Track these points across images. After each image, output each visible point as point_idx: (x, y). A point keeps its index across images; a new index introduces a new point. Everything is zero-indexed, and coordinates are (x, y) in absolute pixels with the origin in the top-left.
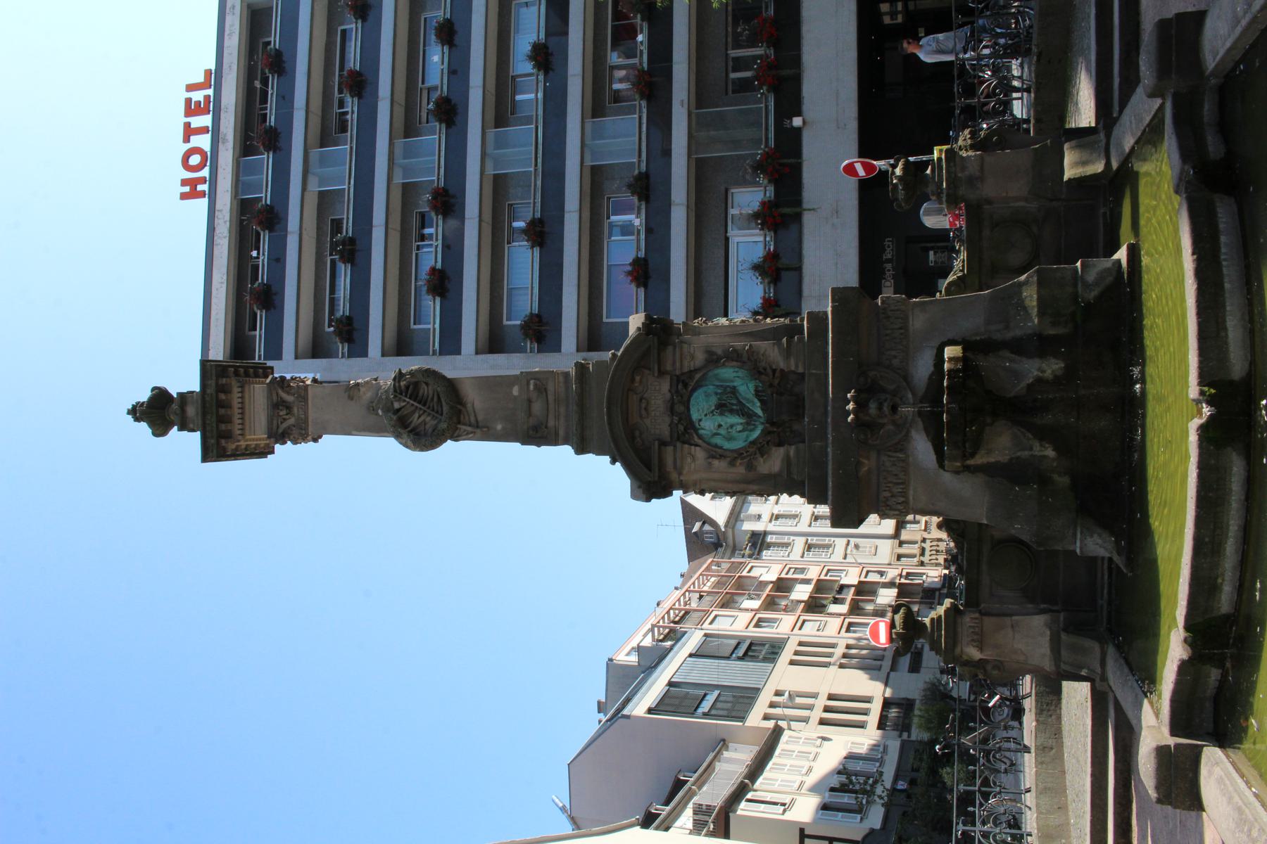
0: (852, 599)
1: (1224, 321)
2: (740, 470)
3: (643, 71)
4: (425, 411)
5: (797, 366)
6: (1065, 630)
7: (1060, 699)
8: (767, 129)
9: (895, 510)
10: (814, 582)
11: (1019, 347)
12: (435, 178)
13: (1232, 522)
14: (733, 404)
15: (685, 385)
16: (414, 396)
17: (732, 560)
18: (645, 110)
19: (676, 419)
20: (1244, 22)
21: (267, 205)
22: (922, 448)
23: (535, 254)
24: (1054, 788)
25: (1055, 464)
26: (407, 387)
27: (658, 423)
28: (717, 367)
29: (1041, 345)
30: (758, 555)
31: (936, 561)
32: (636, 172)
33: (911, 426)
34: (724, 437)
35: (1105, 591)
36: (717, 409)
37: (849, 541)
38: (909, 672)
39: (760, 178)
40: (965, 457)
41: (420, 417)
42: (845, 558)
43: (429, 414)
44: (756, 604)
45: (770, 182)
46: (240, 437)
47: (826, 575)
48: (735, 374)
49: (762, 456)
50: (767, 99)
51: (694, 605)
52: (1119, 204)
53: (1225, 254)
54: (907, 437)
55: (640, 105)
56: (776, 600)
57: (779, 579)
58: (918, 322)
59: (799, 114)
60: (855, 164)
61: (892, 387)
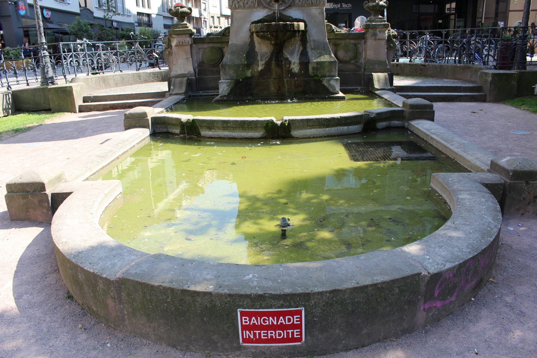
1: (314, 128)
6: (188, 79)
7: (160, 81)
9: (232, 4)
11: (304, 54)
13: (236, 133)
22: (260, 14)
24: (124, 82)
29: (304, 63)
33: (269, 9)
35: (205, 94)
38: (164, 24)
52: (362, 94)
53: (340, 128)
54: (265, 7)
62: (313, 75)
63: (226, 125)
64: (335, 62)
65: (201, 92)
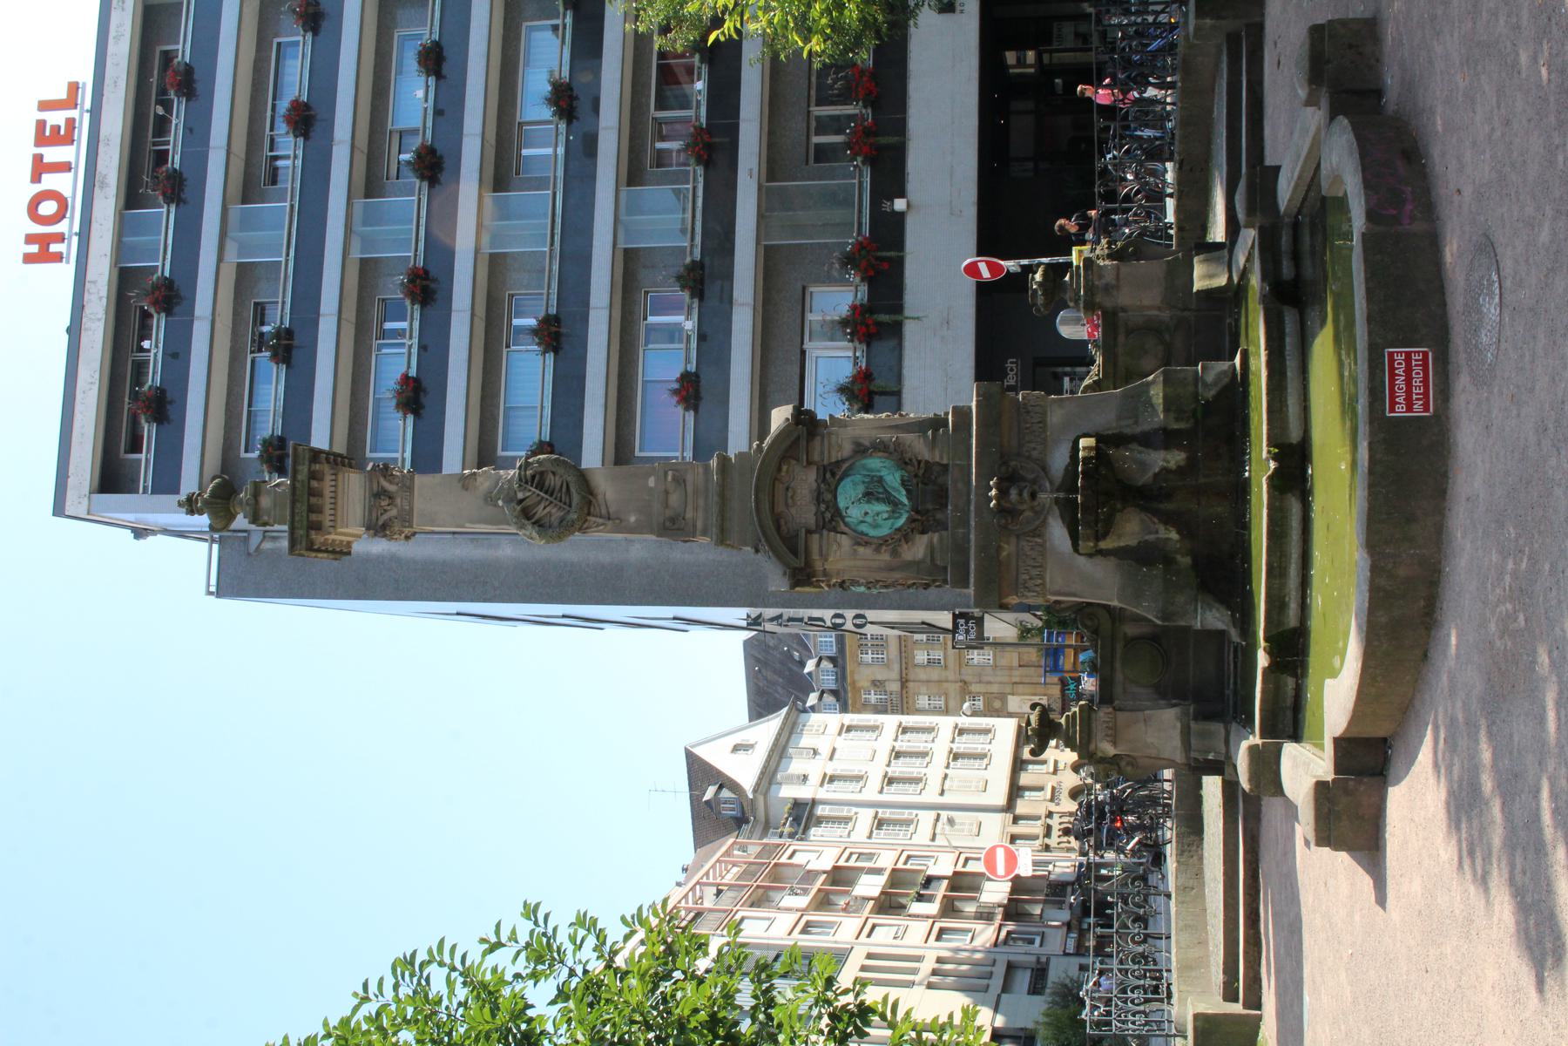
0: (944, 896)
1: (1286, 401)
2: (885, 557)
3: (702, 129)
4: (551, 502)
5: (941, 458)
6: (1196, 719)
7: (1203, 839)
8: (860, 212)
11: (1146, 440)
12: (411, 254)
14: (879, 493)
15: (832, 474)
16: (540, 486)
17: (765, 841)
18: (701, 180)
19: (823, 507)
20: (1292, 184)
21: (166, 278)
22: (1058, 533)
23: (547, 362)
24: (1197, 925)
25: (1178, 546)
26: (533, 477)
27: (803, 512)
28: (864, 458)
29: (1167, 438)
30: (804, 833)
31: (1067, 845)
32: (688, 260)
33: (1048, 513)
34: (871, 525)
35: (1232, 681)
37: (939, 815)
38: (1029, 994)
39: (850, 275)
40: (1097, 539)
41: (545, 508)
42: (933, 839)
43: (556, 505)
44: (803, 901)
45: (863, 280)
46: (331, 530)
47: (905, 863)
48: (882, 465)
49: (907, 543)
50: (861, 176)
51: (708, 903)
52: (1239, 313)
54: (1044, 523)
55: (695, 171)
56: (831, 897)
57: (836, 868)
58: (1055, 417)
59: (902, 195)
61: (1030, 476)
62: (1192, 421)
63: (1276, 571)
64: (1164, 373)
65: (1227, 692)
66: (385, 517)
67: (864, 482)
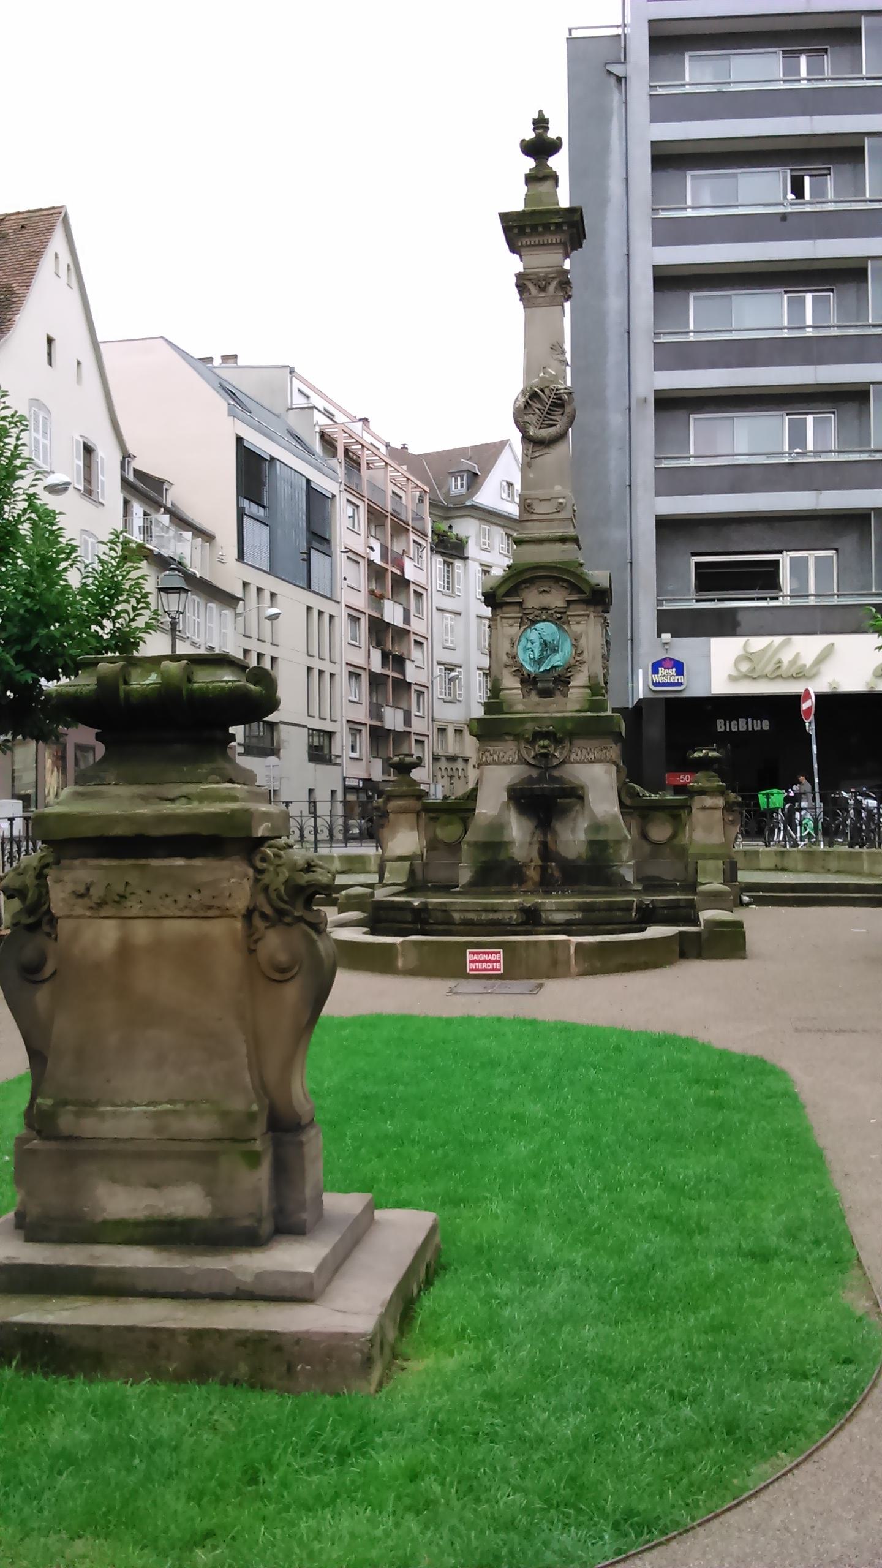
4: (542, 413)
10: (406, 627)
14: (546, 651)
15: (560, 619)
16: (554, 404)
27: (533, 599)
36: (544, 641)
60: (810, 701)
66: (531, 286)
67: (553, 641)
